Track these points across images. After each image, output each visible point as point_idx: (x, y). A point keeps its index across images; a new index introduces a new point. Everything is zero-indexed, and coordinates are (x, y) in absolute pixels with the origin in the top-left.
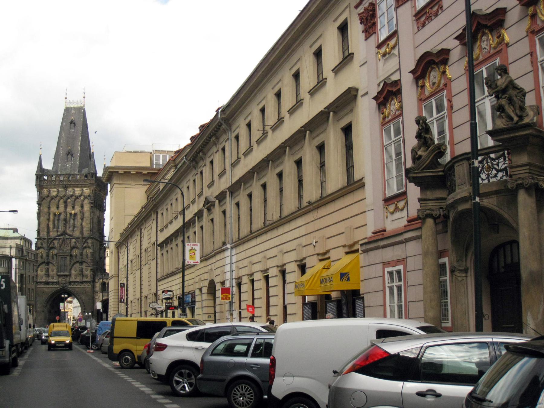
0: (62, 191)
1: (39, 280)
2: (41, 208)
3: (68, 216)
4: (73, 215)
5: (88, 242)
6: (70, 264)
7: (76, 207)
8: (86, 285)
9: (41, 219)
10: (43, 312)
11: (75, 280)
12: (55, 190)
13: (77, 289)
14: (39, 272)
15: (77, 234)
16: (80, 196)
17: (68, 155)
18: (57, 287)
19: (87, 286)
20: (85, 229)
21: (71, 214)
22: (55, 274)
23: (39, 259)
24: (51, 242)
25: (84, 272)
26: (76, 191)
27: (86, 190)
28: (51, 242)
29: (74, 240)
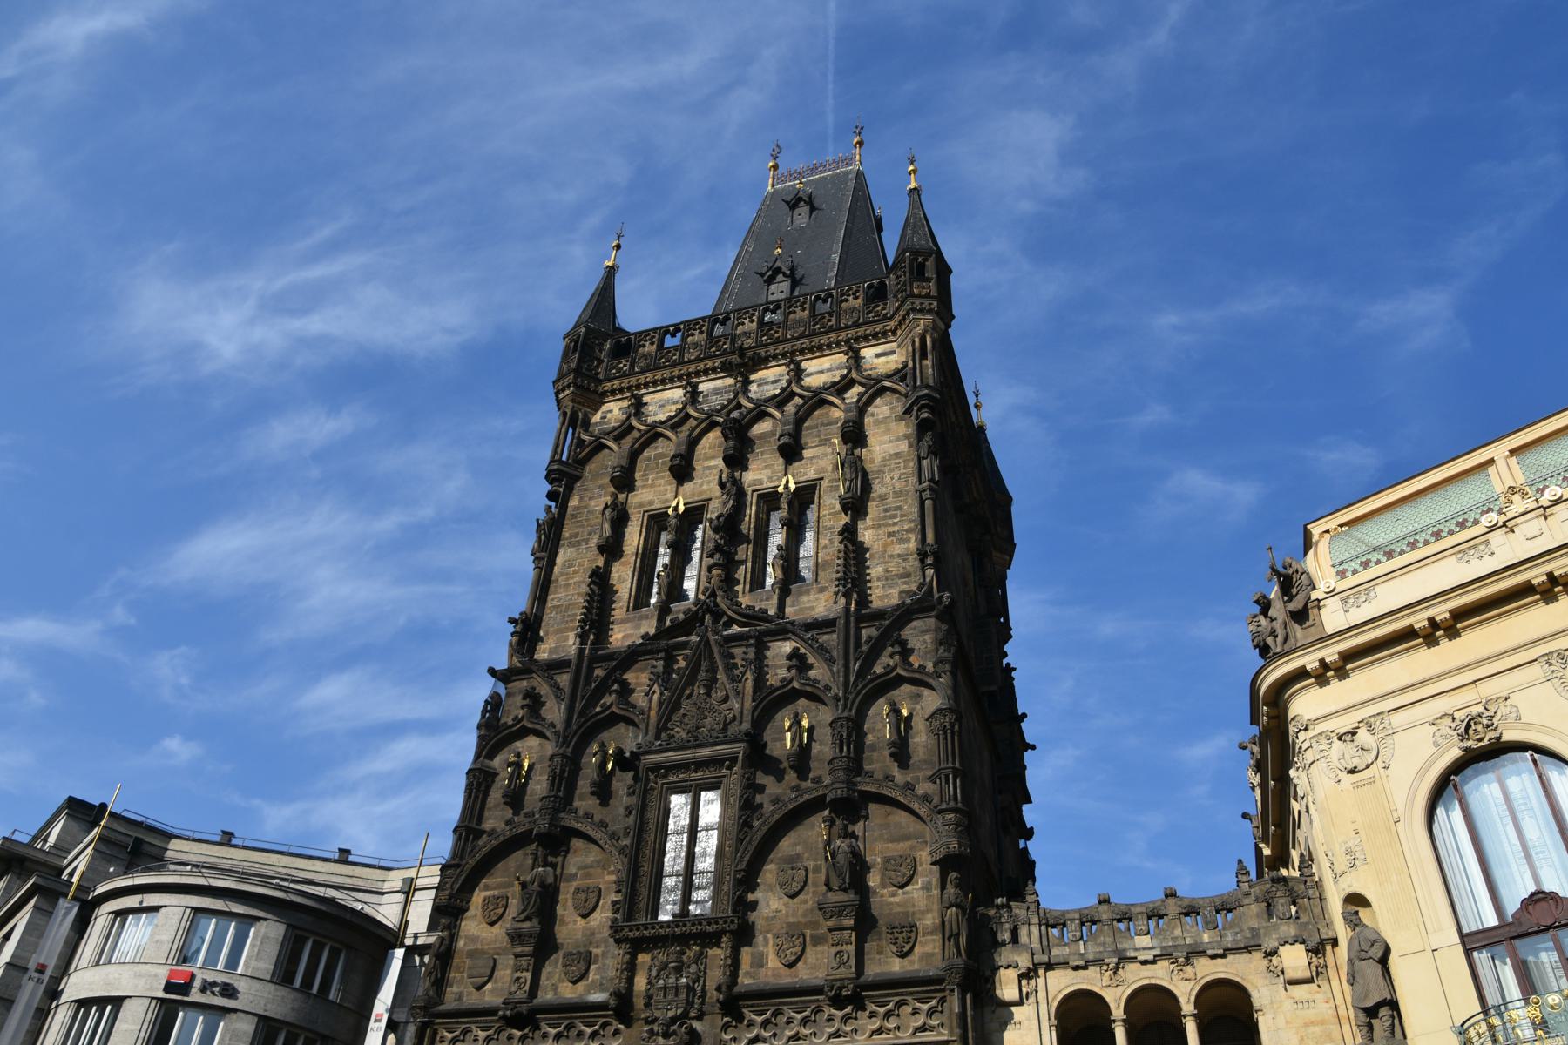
0: (716, 391)
1: (460, 998)
2: (574, 502)
3: (751, 511)
5: (903, 643)
6: (746, 824)
9: (560, 559)
11: (787, 979)
12: (678, 394)
14: (474, 928)
15: (818, 602)
16: (841, 387)
17: (770, 281)
20: (875, 570)
21: (769, 500)
22: (606, 932)
23: (496, 819)
26: (809, 375)
27: (878, 356)
28: (603, 688)
29: (787, 647)
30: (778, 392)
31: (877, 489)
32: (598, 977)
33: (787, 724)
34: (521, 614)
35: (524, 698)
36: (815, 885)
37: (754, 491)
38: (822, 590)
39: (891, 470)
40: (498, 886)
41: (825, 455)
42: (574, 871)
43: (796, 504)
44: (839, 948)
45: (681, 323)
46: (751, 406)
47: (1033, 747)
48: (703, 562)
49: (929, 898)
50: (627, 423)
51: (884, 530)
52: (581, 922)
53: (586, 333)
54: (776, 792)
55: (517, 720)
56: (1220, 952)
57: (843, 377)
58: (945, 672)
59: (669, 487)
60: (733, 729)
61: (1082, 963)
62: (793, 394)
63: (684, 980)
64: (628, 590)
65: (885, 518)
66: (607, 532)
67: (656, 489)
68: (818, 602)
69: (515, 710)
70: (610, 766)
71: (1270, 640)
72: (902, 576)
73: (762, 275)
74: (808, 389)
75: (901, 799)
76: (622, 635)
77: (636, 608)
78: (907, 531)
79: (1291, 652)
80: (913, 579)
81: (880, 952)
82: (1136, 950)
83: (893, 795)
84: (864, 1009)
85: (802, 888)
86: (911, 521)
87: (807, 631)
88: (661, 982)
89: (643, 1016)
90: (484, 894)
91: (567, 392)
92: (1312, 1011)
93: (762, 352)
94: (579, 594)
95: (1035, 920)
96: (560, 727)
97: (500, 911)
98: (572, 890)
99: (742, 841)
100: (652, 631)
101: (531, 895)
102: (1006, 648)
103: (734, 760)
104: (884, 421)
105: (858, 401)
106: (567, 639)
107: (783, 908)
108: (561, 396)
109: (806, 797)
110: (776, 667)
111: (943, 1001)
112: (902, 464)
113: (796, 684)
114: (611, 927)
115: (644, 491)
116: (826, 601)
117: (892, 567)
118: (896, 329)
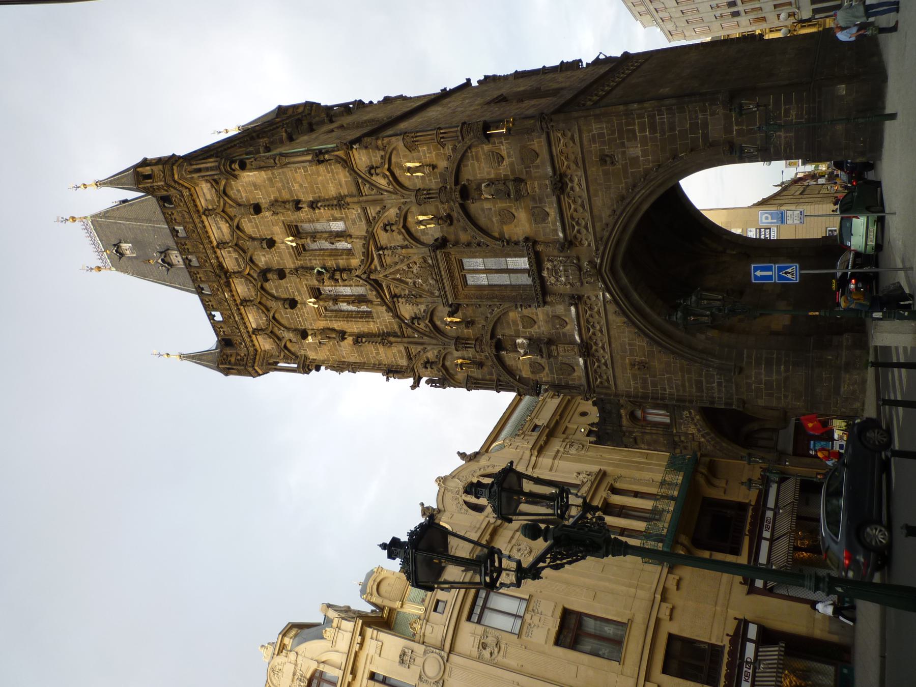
6: (479, 245)
17: (171, 265)
18: (601, 304)
33: (422, 227)
45: (206, 312)
55: (439, 370)
57: (222, 217)
63: (561, 268)
70: (458, 320)
73: (168, 270)
91: (256, 368)
99: (488, 245)
102: (366, 102)
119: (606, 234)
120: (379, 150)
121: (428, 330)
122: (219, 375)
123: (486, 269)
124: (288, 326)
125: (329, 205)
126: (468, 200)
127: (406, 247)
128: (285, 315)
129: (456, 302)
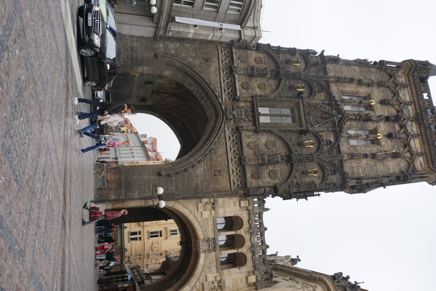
0: (409, 111)
2: (373, 70)
3: (371, 126)
4: (374, 135)
5: (334, 174)
6: (285, 131)
7: (389, 142)
8: (234, 177)
10: (156, 55)
11: (244, 145)
13: (221, 150)
14: (253, 55)
19: (232, 178)
21: (374, 131)
22: (254, 93)
24: (320, 85)
25: (265, 167)
26: (414, 141)
27: (420, 162)
30: (409, 131)
31: (378, 164)
32: (243, 92)
33: (311, 141)
34: (340, 58)
35: (317, 63)
36: (269, 151)
37: (377, 126)
38: (348, 149)
39: (384, 168)
40: (265, 61)
41: (389, 147)
42: (270, 82)
43: (373, 139)
44: (253, 159)
46: (404, 123)
47: (297, 201)
48: (356, 112)
49: (266, 183)
50: (398, 84)
51: (366, 166)
52: (256, 86)
53: (429, 68)
54: (293, 139)
56: (254, 260)
58: (326, 186)
59: (378, 99)
60: (309, 125)
61: (250, 223)
62: (408, 136)
63: (244, 117)
64: (347, 89)
65: (370, 166)
66: (365, 81)
67: (378, 96)
68: (344, 148)
69: (313, 60)
70: (298, 90)
71: (337, 280)
72: (353, 172)
74: (410, 141)
75: (292, 175)
76: (334, 89)
77: (342, 92)
78: (366, 173)
79: (335, 288)
80: (352, 175)
81: (252, 170)
82: (254, 237)
83: (293, 173)
84: (238, 167)
85: (268, 148)
86: (369, 174)
87: (337, 145)
88: (243, 111)
89: (234, 106)
90: (263, 57)
91: (409, 64)
92: (240, 282)
93: (422, 126)
94: (346, 75)
95: (260, 211)
96: (309, 75)
97: (258, 62)
98: (265, 82)
99: (280, 130)
100: (336, 99)
101: (264, 71)
103: (301, 127)
104: (399, 165)
105: (406, 157)
106: (333, 73)
107: (262, 143)
108: (408, 62)
109: (292, 148)
110: (327, 137)
111: (241, 188)
112: (386, 171)
113: (322, 143)
114: (256, 95)
115: (377, 92)
116: (345, 150)
117: (355, 169)
118: (430, 168)
119: (220, 133)
120: (328, 183)
121: (314, 84)
122: (431, 62)
123: (281, 117)
124: (387, 89)
125: (358, 156)
126: (288, 155)
127: (321, 132)
128: (390, 96)
129: (298, 100)
